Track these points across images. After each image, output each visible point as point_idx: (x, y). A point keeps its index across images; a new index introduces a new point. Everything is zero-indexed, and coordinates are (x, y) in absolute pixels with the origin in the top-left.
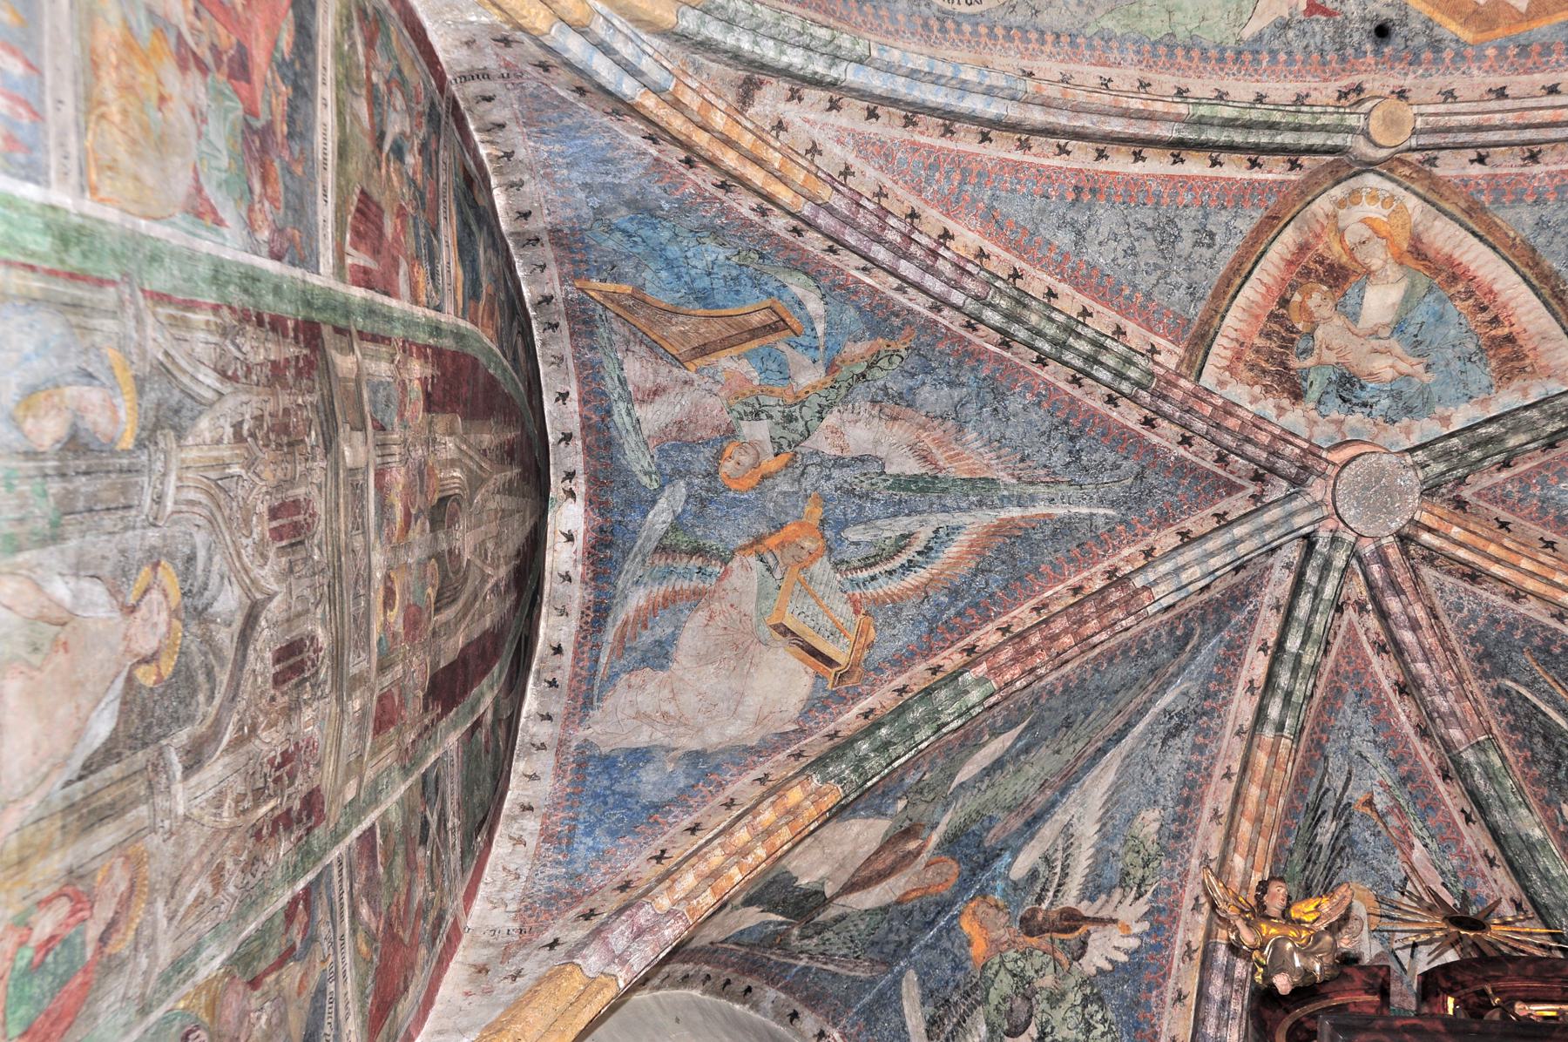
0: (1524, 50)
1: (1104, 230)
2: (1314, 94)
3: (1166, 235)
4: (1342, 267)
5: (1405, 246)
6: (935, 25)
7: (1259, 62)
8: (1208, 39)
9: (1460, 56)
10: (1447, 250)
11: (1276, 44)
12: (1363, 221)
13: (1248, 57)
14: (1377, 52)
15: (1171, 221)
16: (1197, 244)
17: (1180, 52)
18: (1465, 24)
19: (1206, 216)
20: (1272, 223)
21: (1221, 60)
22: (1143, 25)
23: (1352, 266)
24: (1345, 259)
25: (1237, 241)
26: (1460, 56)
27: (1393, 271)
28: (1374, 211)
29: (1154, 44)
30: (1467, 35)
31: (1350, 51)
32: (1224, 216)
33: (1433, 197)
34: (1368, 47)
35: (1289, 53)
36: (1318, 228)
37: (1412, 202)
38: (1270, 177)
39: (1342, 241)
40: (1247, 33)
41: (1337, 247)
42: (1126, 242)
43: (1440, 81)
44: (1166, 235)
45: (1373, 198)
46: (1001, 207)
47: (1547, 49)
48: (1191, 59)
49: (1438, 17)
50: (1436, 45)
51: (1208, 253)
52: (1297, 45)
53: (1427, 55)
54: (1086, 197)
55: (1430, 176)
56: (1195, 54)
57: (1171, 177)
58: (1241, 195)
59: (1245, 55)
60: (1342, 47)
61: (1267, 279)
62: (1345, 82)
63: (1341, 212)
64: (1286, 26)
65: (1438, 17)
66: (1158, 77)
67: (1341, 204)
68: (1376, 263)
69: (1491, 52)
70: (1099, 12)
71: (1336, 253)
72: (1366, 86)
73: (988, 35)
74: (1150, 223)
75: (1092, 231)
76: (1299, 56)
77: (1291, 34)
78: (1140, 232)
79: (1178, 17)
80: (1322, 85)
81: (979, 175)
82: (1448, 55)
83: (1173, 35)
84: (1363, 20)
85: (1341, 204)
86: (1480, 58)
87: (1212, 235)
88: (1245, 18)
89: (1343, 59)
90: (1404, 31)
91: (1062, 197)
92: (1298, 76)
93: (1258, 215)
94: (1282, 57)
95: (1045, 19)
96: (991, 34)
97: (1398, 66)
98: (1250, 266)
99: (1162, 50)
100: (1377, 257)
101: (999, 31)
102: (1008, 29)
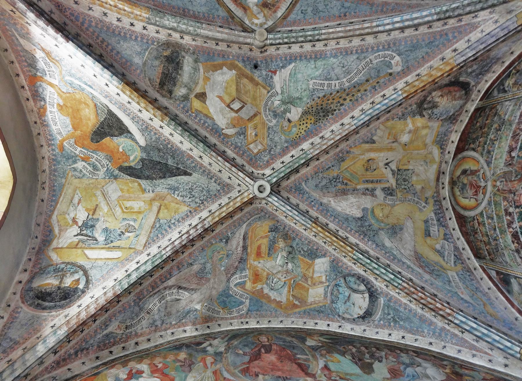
0: (223, 56)
1: (335, 9)
2: (274, 50)
3: (316, 11)
4: (264, 7)
5: (248, 11)
6: (392, 45)
7: (290, 57)
8: (305, 61)
9: (238, 57)
10: (238, 9)
11: (285, 62)
12: (258, 19)
13: (293, 58)
14: (257, 61)
15: (315, 14)
16: (307, 10)
17: (313, 57)
18: (237, 65)
19: (304, 17)
20: (285, 17)
21: (301, 56)
22: (324, 62)
23: (261, 7)
24: (263, 9)
25: (294, 12)
26: (238, 57)
27: (251, 5)
28: (256, 21)
29: (321, 57)
30: (237, 62)
31: (264, 62)
32: (299, 18)
33: (242, 23)
34: (259, 63)
35: (281, 60)
36: (271, 17)
37: (247, 22)
38: (286, 29)
39: (264, 14)
40: (293, 64)
41: (266, 12)
42: (328, 7)
43: (242, 52)
44: (316, 11)
45: (256, 24)
46: (368, 7)
47: (219, 55)
48: (310, 55)
49: (244, 68)
50: (244, 61)
51: (303, 8)
52: (279, 62)
53: (246, 59)
54: (342, 15)
55: (243, 28)
56: (309, 57)
57: (316, 24)
58: (294, 23)
59: (293, 58)
60: (266, 63)
61: (285, 3)
62: (265, 54)
63: (264, 21)
64: (282, 67)
65: (244, 68)
66: (321, 49)
67: (265, 23)
68: (255, 8)
69: (231, 57)
70: (338, 63)
71: (266, 11)
72: (259, 53)
73: (374, 47)
74: (321, 13)
75: (339, 8)
76: (279, 60)
77: (281, 65)
78: (324, 10)
79: (313, 66)
80: (272, 53)
81: (377, 12)
82: (241, 58)
83: (315, 61)
84: (261, 70)
85: (265, 23)
86: (233, 56)
87: (302, 13)
88: (294, 68)
89: (266, 60)
90: (251, 66)
91: (350, 13)
92: (279, 55)
93: (289, 19)
94: (283, 59)
95: (355, 57)
96: (373, 48)
97: (252, 57)
98: (290, 6)
99: (318, 57)
100: (255, 9)
101: (370, 50)
102: (367, 51)
